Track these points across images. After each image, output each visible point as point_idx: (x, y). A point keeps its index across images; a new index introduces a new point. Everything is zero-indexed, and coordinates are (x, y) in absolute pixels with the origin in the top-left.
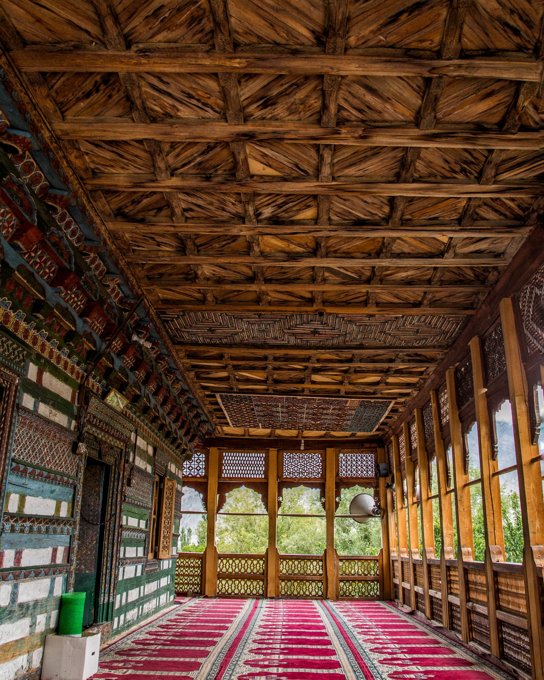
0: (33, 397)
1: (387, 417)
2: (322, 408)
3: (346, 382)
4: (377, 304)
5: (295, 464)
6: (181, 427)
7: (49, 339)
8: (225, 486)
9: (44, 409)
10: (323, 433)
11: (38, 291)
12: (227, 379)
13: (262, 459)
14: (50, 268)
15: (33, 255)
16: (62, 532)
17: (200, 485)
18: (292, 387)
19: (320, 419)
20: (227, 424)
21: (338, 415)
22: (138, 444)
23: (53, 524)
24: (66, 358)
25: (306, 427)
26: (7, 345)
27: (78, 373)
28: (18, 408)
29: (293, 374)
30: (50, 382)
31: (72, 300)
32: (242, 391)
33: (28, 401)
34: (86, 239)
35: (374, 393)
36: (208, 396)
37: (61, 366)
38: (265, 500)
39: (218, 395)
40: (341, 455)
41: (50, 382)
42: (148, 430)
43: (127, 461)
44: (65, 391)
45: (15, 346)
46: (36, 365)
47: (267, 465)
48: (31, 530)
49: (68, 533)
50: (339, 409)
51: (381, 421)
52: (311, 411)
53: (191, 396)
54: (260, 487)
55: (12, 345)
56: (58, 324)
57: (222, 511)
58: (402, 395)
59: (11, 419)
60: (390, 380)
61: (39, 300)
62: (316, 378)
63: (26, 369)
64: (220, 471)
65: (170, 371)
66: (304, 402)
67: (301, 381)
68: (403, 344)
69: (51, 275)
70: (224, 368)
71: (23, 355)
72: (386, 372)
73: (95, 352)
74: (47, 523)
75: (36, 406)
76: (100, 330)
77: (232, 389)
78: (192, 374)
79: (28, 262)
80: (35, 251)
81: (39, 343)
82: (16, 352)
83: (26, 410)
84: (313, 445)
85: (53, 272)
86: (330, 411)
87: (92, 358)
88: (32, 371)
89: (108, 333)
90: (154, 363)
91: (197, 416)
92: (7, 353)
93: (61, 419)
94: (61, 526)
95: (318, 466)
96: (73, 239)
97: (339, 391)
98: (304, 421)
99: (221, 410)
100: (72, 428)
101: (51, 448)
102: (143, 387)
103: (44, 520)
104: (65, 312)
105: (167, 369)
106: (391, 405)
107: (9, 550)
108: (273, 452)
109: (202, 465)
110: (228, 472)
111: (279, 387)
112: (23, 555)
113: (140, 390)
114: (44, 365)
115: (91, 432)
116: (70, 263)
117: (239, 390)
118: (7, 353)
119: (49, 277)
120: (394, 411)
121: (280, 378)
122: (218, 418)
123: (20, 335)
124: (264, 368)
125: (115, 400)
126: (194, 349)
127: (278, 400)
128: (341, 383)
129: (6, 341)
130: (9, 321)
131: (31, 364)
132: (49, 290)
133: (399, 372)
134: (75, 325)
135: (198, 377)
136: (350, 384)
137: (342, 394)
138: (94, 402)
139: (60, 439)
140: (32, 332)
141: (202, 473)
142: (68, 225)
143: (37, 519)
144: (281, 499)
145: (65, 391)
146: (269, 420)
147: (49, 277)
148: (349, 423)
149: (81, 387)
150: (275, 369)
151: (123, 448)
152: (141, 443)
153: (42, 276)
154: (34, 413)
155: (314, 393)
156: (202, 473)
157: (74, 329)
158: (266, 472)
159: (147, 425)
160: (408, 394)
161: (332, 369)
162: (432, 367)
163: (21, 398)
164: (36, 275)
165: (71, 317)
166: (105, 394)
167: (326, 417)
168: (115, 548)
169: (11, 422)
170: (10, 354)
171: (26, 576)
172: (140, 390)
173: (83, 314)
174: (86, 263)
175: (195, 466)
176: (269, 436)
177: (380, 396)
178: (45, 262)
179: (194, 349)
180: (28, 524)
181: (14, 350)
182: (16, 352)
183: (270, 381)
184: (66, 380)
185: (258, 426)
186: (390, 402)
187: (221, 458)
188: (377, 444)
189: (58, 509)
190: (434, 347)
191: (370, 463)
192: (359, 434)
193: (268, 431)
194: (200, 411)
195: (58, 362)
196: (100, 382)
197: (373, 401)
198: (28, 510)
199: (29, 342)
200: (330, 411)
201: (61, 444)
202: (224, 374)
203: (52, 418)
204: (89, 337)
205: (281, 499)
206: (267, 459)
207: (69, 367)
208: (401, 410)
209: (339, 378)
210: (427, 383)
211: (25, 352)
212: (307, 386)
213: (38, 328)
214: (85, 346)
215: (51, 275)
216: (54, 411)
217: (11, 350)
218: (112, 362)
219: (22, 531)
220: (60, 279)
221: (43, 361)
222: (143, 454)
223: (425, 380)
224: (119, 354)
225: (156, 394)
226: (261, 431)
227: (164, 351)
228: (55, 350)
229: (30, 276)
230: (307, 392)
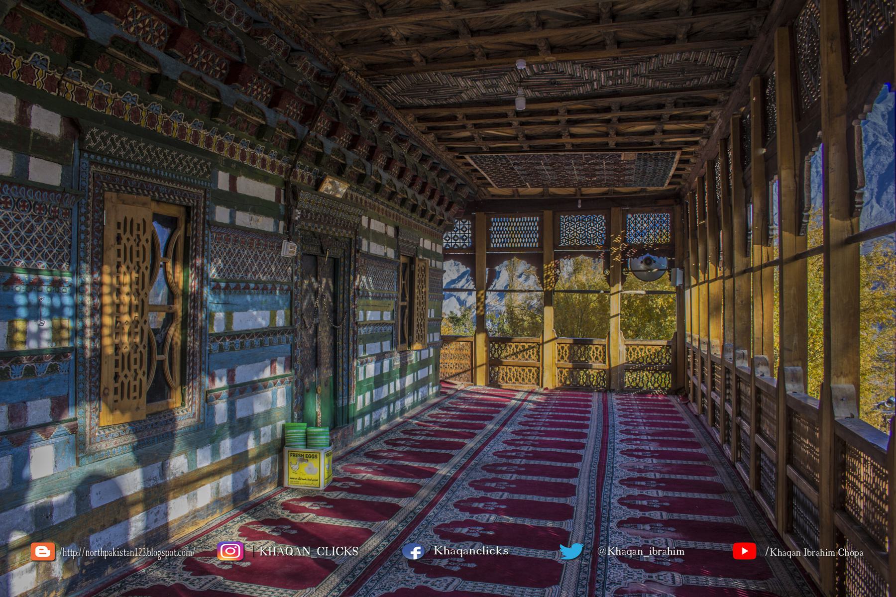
0: (228, 207)
2: (593, 164)
5: (574, 228)
6: (431, 197)
7: (237, 140)
9: (243, 219)
10: (606, 189)
11: (212, 94)
14: (220, 65)
15: (196, 56)
16: (280, 343)
21: (615, 170)
22: (372, 227)
23: (268, 335)
24: (262, 155)
26: (187, 162)
27: (281, 167)
28: (209, 225)
30: (247, 186)
31: (256, 93)
32: (492, 150)
33: (222, 214)
34: (255, 22)
36: (458, 157)
37: (257, 166)
39: (467, 157)
40: (629, 216)
41: (247, 186)
42: (385, 208)
43: (358, 251)
44: (267, 192)
45: (196, 160)
46: (226, 172)
48: (242, 346)
49: (288, 342)
50: (615, 164)
51: (671, 174)
53: (435, 161)
55: (192, 160)
56: (245, 121)
59: (203, 237)
61: (215, 103)
63: (215, 180)
65: (400, 140)
69: (224, 72)
71: (207, 167)
73: (296, 141)
74: (260, 336)
75: (232, 217)
76: (298, 115)
78: (432, 137)
79: (193, 66)
80: (198, 52)
81: (227, 147)
82: (198, 167)
83: (221, 225)
84: (592, 205)
85: (225, 68)
87: (295, 147)
88: (223, 181)
89: (309, 116)
90: (377, 134)
91: (451, 180)
92: (187, 170)
93: (266, 224)
94: (278, 336)
96: (240, 26)
98: (578, 178)
100: (281, 231)
101: (256, 258)
102: (368, 164)
103: (256, 334)
104: (250, 108)
105: (397, 137)
107: (220, 370)
108: (548, 214)
109: (469, 234)
112: (236, 372)
113: (364, 169)
114: (236, 170)
115: (306, 228)
116: (240, 54)
118: (187, 170)
119: (222, 74)
123: (201, 145)
125: (335, 187)
126: (421, 112)
127: (538, 158)
129: (184, 158)
130: (186, 133)
131: (220, 173)
132: (224, 88)
134: (264, 118)
135: (439, 139)
138: (304, 196)
139: (266, 245)
140: (216, 138)
142: (229, 13)
143: (248, 334)
145: (267, 192)
146: (535, 178)
147: (222, 74)
148: (632, 178)
149: (286, 183)
151: (353, 236)
152: (377, 226)
153: (213, 76)
154: (232, 226)
157: (264, 123)
159: (383, 203)
163: (213, 212)
164: (205, 78)
165: (258, 111)
166: (319, 183)
167: (602, 172)
168: (351, 348)
169: (203, 241)
170: (192, 170)
171: (242, 392)
172: (364, 169)
173: (273, 103)
174: (263, 47)
175: (460, 234)
176: (543, 196)
178: (213, 60)
179: (421, 112)
180: (238, 340)
181: (195, 164)
182: (198, 167)
183: (521, 138)
184: (266, 179)
185: (525, 186)
187: (489, 224)
188: (672, 200)
189: (273, 318)
194: (452, 174)
195: (254, 162)
196: (310, 170)
198: (236, 327)
199: (213, 150)
201: (268, 249)
203: (253, 225)
204: (286, 126)
206: (541, 224)
207: (268, 164)
210: (716, 130)
211: (209, 164)
213: (221, 132)
214: (283, 137)
215: (224, 72)
216: (255, 217)
217: (192, 165)
218: (321, 145)
219: (232, 349)
220: (234, 74)
221: (234, 166)
222: (379, 238)
223: (713, 126)
224: (330, 135)
225: (387, 168)
227: (387, 120)
228: (249, 150)
229: (199, 82)
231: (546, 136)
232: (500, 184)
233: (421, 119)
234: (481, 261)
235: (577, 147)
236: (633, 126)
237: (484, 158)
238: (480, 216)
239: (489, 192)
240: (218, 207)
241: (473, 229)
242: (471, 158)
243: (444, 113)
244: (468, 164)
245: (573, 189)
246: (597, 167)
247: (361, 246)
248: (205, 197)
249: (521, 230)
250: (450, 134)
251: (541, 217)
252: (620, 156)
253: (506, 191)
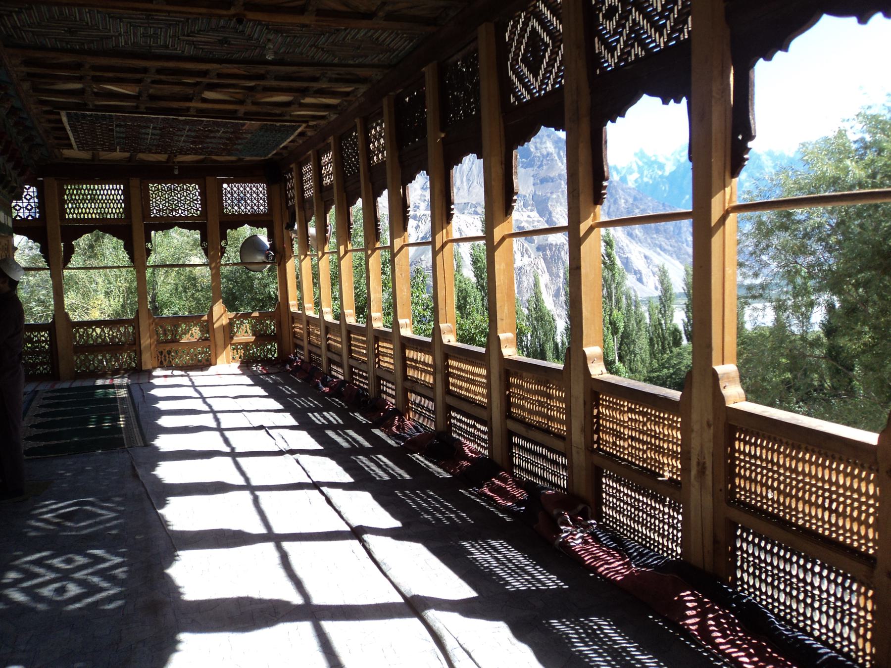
1: (292, 141)
2: (209, 131)
3: (249, 101)
4: (320, 13)
5: (162, 197)
12: (82, 92)
13: (120, 192)
18: (175, 105)
19: (201, 143)
20: (70, 146)
21: (227, 139)
25: (182, 152)
32: (98, 108)
35: (280, 115)
40: (225, 186)
50: (232, 133)
52: (193, 134)
53: (25, 116)
58: (314, 117)
60: (308, 100)
66: (186, 122)
67: (189, 99)
68: (336, 61)
70: (79, 79)
72: (304, 92)
77: (86, 104)
78: (26, 86)
86: (219, 135)
95: (196, 200)
97: (236, 111)
98: (181, 144)
99: (64, 129)
106: (299, 130)
117: (96, 106)
120: (302, 134)
122: (56, 138)
124: (139, 81)
128: (241, 102)
133: (321, 93)
136: (254, 103)
137: (240, 114)
148: (239, 147)
150: (153, 82)
160: (323, 117)
162: (363, 89)
167: (213, 140)
177: (288, 118)
185: (115, 150)
186: (299, 126)
188: (273, 173)
190: (372, 66)
191: (261, 195)
192: (248, 158)
193: (127, 155)
197: (278, 124)
200: (219, 135)
202: (78, 86)
208: (309, 134)
209: (240, 96)
226: (118, 155)
230: (192, 112)
231: (174, 98)
232: (82, 146)
233: (27, 63)
234: (57, 238)
235: (201, 113)
236: (272, 96)
237: (84, 116)
243: (67, 59)
244: (60, 121)
245: (166, 156)
250: (53, 84)
252: (244, 125)
253: (85, 155)
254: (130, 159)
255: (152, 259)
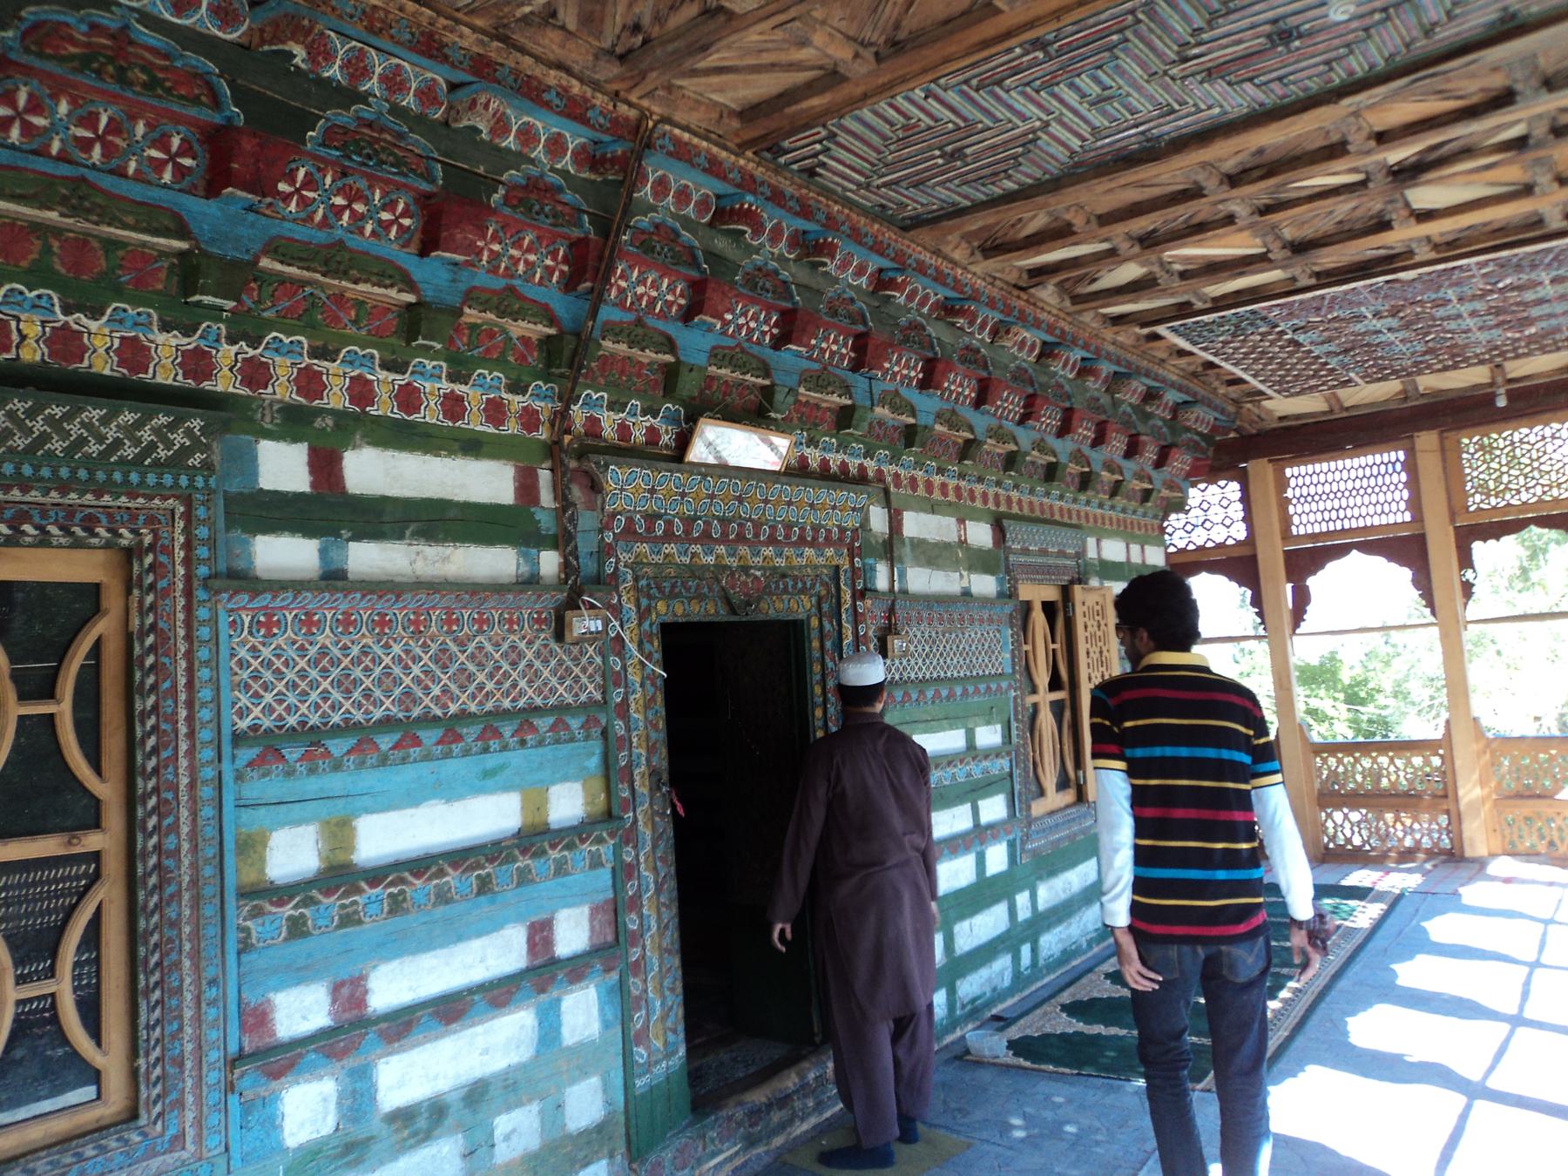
8: (1306, 559)
17: (1239, 564)
29: (1342, 208)
38: (1423, 582)
47: (1413, 484)
54: (1405, 547)
57: (1304, 627)
62: (1424, 196)
64: (1286, 521)
66: (1434, 283)
67: (1382, 225)
109: (1237, 510)
110: (1307, 521)
111: (1329, 258)
117: (1214, 300)
121: (1308, 232)
141: (1240, 532)
144: (1469, 575)
155: (1451, 248)
156: (1240, 532)
158: (1415, 504)
161: (1467, 152)
187: (1283, 484)
205: (1469, 575)
206: (1411, 467)
212: (1401, 235)
232: (1284, 388)
238: (1260, 468)
239: (1269, 412)
240: (259, 538)
241: (1245, 499)
242: (1173, 329)
246: (1529, 296)
247: (873, 578)
248: (188, 517)
249: (1349, 489)
251: (1411, 452)
254: (1405, 395)
255: (1474, 610)
